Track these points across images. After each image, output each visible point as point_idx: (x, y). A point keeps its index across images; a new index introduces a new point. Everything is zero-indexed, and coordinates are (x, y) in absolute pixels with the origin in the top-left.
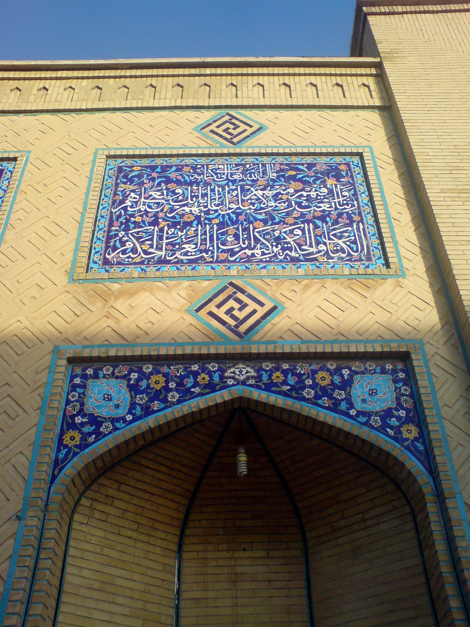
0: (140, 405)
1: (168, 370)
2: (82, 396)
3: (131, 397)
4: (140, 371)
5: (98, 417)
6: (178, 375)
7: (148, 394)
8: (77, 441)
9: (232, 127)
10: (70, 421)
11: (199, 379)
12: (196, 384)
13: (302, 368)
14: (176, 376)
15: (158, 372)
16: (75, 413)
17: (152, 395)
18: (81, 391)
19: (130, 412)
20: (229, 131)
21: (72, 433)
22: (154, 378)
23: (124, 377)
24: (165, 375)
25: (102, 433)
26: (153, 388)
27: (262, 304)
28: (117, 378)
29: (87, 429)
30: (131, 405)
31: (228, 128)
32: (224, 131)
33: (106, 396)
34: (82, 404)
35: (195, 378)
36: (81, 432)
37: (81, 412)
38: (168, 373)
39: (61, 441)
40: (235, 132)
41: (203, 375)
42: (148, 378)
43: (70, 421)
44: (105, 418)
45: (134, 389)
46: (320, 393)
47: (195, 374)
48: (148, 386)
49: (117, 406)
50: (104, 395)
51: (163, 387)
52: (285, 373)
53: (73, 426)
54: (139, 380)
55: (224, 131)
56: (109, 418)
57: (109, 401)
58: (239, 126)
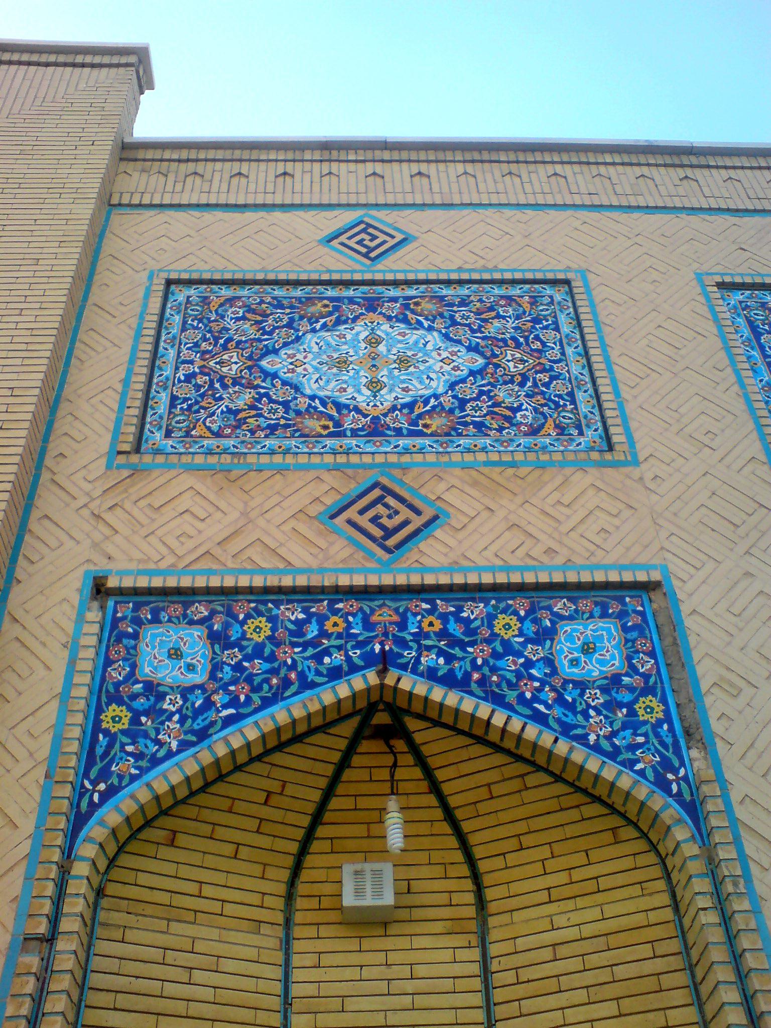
0: (229, 665)
1: (275, 612)
2: (132, 651)
3: (214, 653)
4: (230, 614)
5: (159, 685)
6: (293, 618)
7: (242, 649)
8: (125, 724)
9: (368, 237)
10: (112, 690)
11: (328, 626)
12: (323, 634)
13: (474, 611)
14: (290, 620)
15: (260, 614)
16: (121, 679)
17: (249, 650)
18: (132, 642)
19: (213, 676)
20: (370, 238)
21: (114, 710)
22: (251, 625)
23: (201, 622)
24: (272, 619)
25: (166, 710)
26: (250, 639)
27: (418, 512)
28: (191, 623)
29: (141, 703)
30: (213, 665)
31: (363, 240)
32: (358, 243)
33: (172, 652)
34: (134, 666)
35: (321, 624)
36: (130, 708)
37: (131, 677)
38: (277, 616)
39: (97, 722)
40: (373, 244)
41: (334, 619)
42: (243, 623)
43: (112, 690)
44: (172, 688)
45: (216, 638)
46: (500, 649)
47: (322, 619)
48: (243, 637)
49: (191, 668)
50: (169, 651)
51: (268, 638)
52: (444, 618)
53: (116, 698)
54: (226, 626)
55: (358, 243)
56: (178, 687)
57: (177, 659)
58: (377, 237)
